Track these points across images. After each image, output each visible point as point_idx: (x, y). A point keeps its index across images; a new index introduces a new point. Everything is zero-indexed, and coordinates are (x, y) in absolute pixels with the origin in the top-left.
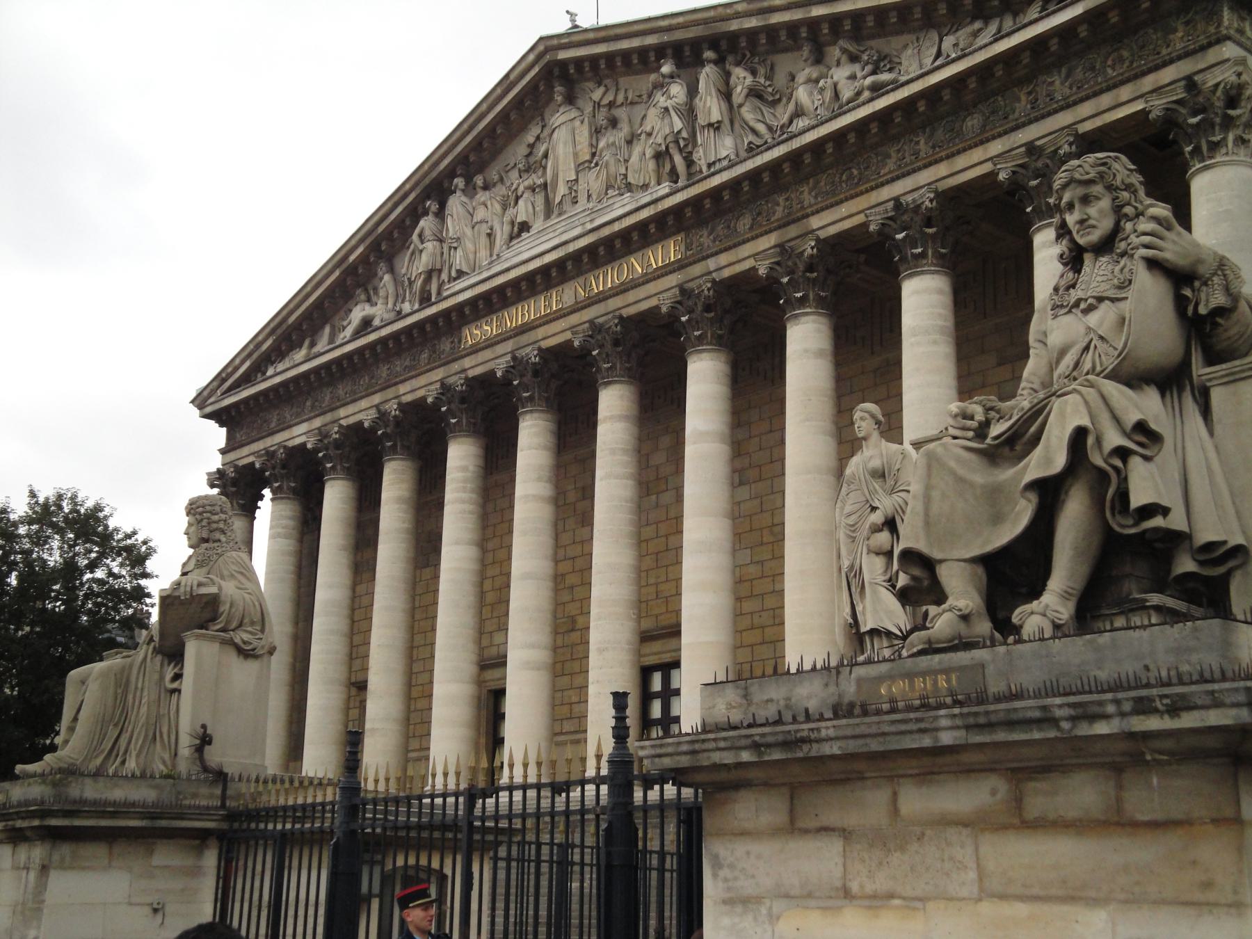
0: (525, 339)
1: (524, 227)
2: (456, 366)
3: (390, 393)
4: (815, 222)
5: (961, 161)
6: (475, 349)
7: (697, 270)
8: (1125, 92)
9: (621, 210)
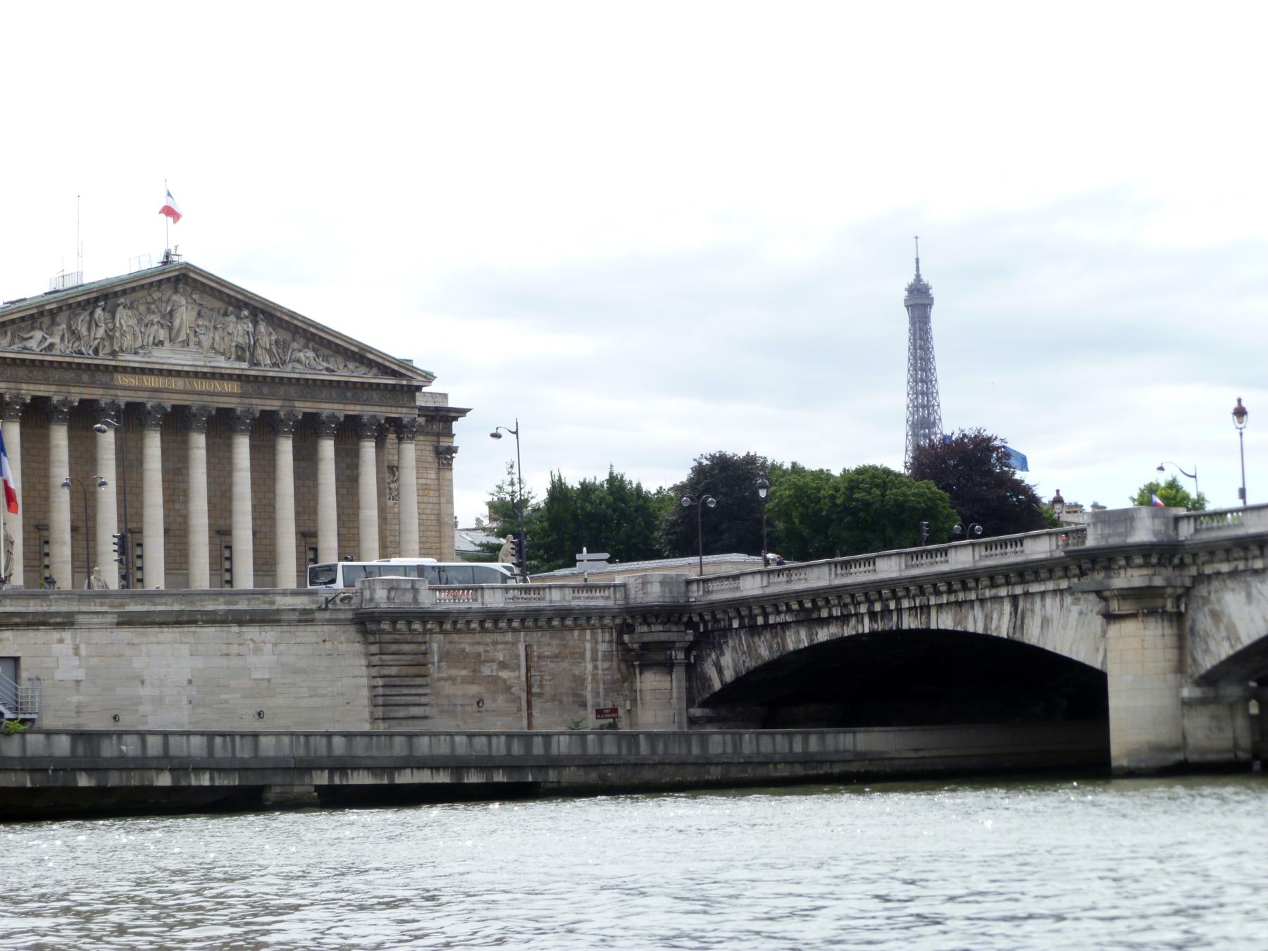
0: (156, 395)
1: (161, 343)
2: (112, 392)
3: (64, 389)
4: (297, 404)
5: (348, 407)
6: (125, 388)
7: (247, 401)
8: (394, 410)
9: (222, 363)
